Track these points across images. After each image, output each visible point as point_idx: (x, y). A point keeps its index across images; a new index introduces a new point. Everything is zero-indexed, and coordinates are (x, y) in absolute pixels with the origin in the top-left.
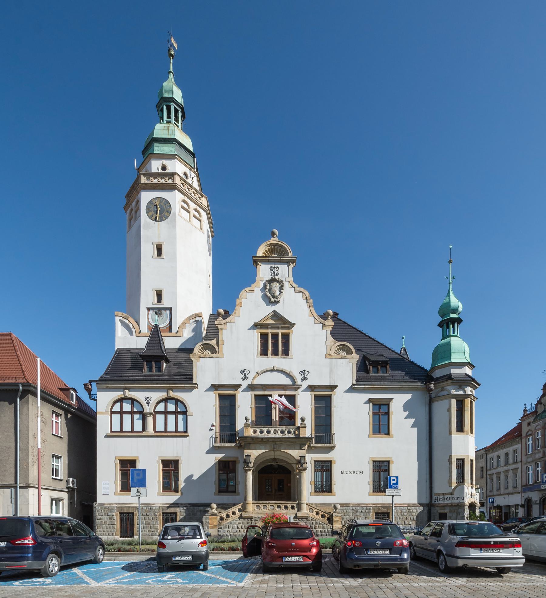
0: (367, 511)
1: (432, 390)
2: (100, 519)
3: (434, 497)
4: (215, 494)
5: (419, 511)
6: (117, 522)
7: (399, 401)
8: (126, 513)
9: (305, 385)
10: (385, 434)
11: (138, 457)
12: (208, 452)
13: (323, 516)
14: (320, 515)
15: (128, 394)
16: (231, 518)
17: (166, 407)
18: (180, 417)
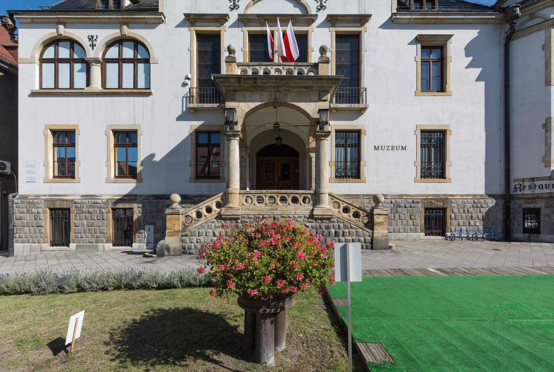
0: (413, 205)
1: (517, 17)
2: (21, 219)
3: (513, 184)
4: (191, 181)
5: (491, 205)
6: (46, 223)
7: (460, 40)
8: (58, 209)
9: (322, 16)
10: (438, 91)
11: (77, 126)
12: (179, 119)
13: (356, 215)
14: (351, 213)
15: (63, 31)
16: (203, 217)
17: (120, 52)
18: (141, 66)
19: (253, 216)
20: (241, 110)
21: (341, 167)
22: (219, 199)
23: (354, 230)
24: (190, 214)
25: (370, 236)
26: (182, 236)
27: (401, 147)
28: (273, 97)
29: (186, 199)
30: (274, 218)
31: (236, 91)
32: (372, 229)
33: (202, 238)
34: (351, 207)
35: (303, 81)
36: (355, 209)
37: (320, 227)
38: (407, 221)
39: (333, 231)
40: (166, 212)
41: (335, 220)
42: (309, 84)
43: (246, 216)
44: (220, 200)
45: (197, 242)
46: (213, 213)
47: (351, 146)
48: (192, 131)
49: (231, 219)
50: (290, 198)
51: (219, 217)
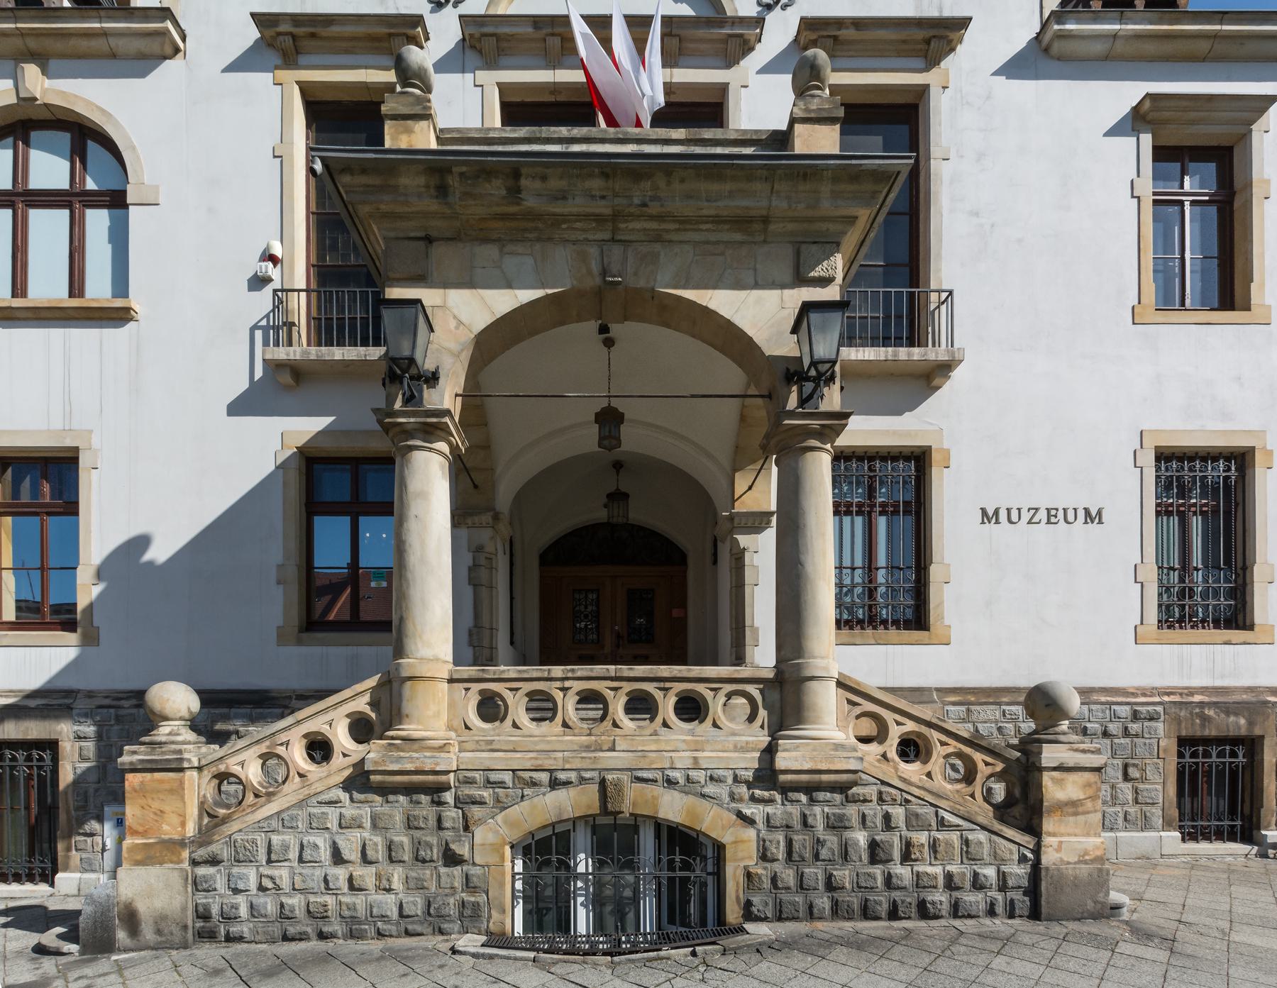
19: (507, 778)
20: (453, 324)
21: (854, 586)
22: (362, 705)
23: (954, 837)
24: (236, 769)
25: (1023, 859)
26: (194, 863)
27: (1081, 514)
28: (595, 267)
29: (224, 710)
30: (603, 782)
31: (429, 240)
32: (1033, 828)
33: (282, 874)
34: (935, 735)
35: (728, 186)
36: (954, 746)
37: (805, 823)
38: (1113, 787)
39: (861, 838)
40: (125, 759)
41: (871, 791)
42: (755, 200)
43: (477, 775)
44: (367, 710)
45: (262, 888)
46: (337, 760)
47: (890, 510)
48: (288, 453)
49: (410, 790)
50: (672, 700)
51: (359, 781)
